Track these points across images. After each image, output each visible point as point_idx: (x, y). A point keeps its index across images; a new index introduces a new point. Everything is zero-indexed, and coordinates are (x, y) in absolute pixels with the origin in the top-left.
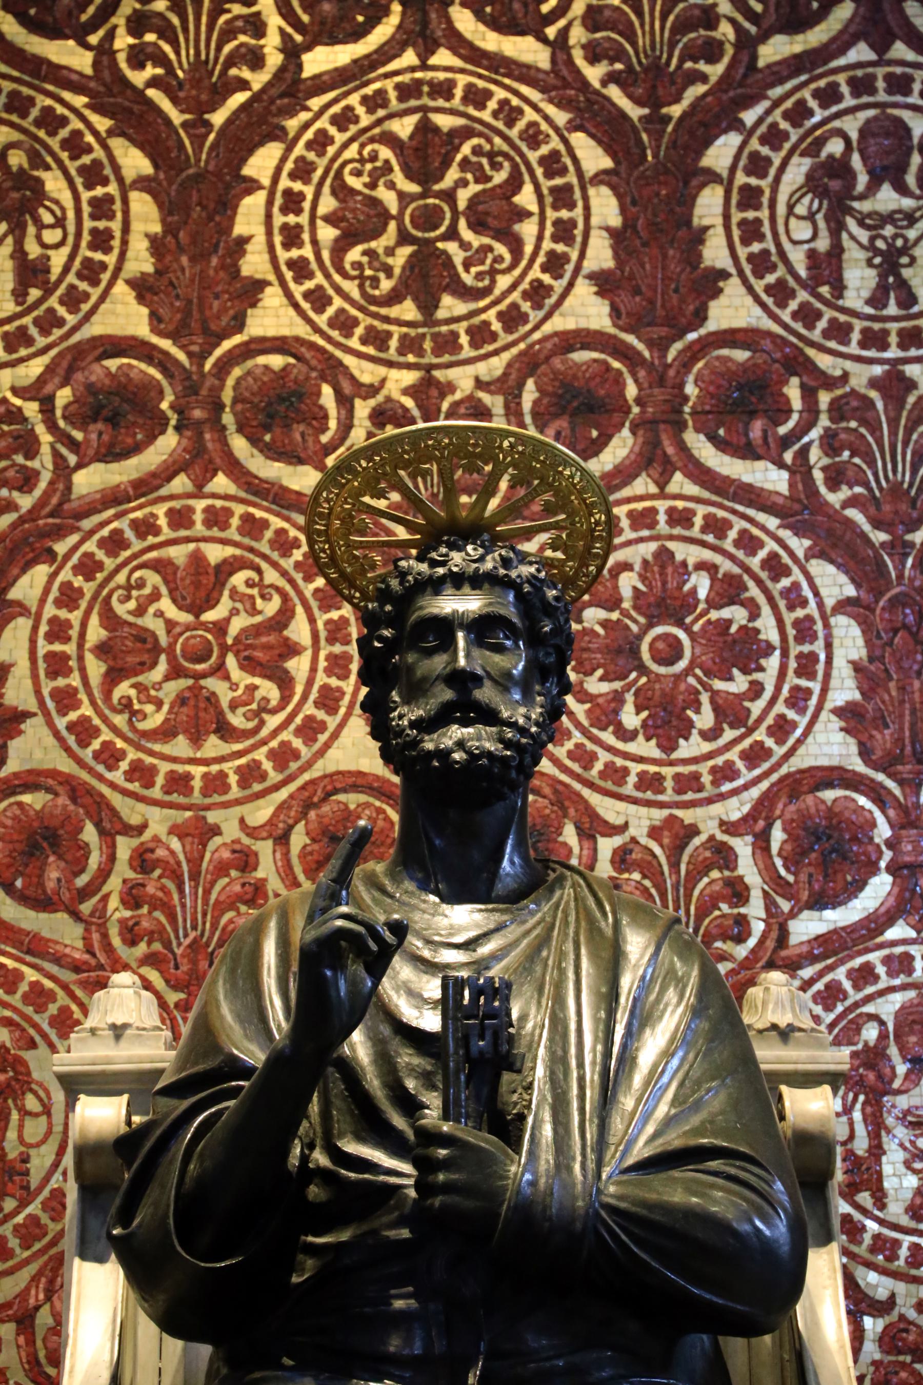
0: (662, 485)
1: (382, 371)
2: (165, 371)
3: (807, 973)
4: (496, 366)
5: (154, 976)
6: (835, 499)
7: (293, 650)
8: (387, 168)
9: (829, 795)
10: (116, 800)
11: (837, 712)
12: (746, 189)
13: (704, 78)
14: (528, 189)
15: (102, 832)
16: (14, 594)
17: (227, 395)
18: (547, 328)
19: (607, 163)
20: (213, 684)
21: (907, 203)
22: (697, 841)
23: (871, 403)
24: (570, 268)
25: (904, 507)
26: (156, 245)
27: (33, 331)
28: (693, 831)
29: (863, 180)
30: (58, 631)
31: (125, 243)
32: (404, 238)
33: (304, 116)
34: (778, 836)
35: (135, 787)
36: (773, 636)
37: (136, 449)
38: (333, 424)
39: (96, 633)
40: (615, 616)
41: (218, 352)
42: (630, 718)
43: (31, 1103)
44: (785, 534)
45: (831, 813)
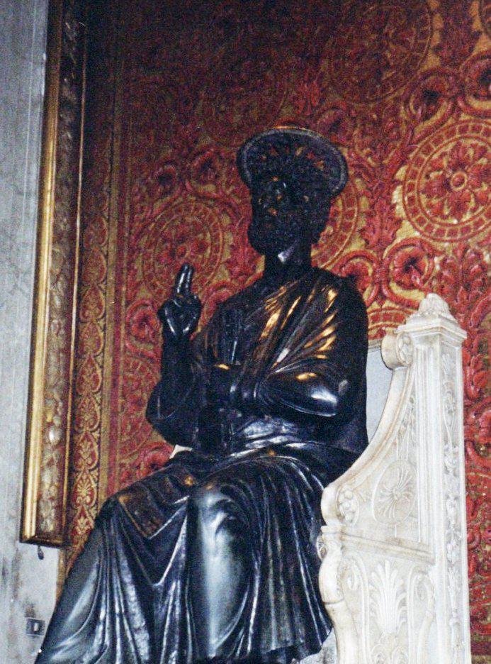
40: (441, 172)
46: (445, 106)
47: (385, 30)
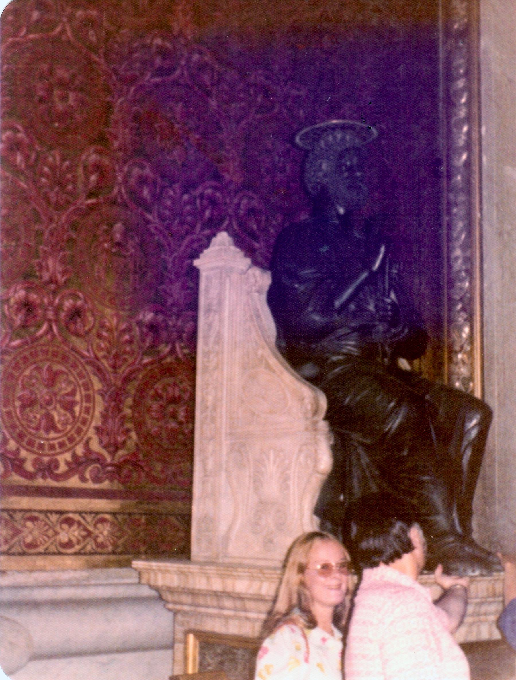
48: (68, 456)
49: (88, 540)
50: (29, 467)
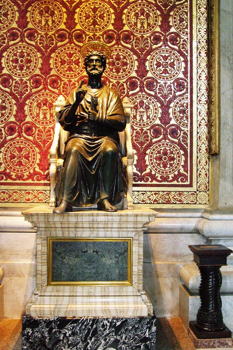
0: (118, 46)
1: (89, 33)
2: (67, 33)
3: (131, 97)
4: (101, 33)
5: (65, 96)
6: (136, 48)
7: (80, 62)
8: (91, 11)
9: (134, 79)
10: (62, 78)
11: (135, 71)
12: (128, 15)
13: (124, 3)
14: (105, 14)
15: (60, 81)
16: (51, 56)
17: (73, 35)
18: (107, 29)
19: (114, 12)
20: (71, 66)
21: (144, 18)
22: (120, 84)
23: (139, 39)
24: (109, 23)
25: (142, 50)
26: (67, 19)
27: (54, 28)
28: (120, 83)
29: (140, 15)
30: (56, 60)
31: (63, 18)
32: (92, 19)
33: (82, 5)
34: (128, 83)
35: (63, 76)
36: (129, 63)
37: (64, 41)
38: (84, 39)
39: (60, 60)
41: (72, 31)
42: (114, 71)
43: (53, 108)
44: (130, 52)
45: (134, 81)
46: (114, 42)
47: (97, 13)
48: (28, 173)
49: (36, 198)
50: (14, 177)
